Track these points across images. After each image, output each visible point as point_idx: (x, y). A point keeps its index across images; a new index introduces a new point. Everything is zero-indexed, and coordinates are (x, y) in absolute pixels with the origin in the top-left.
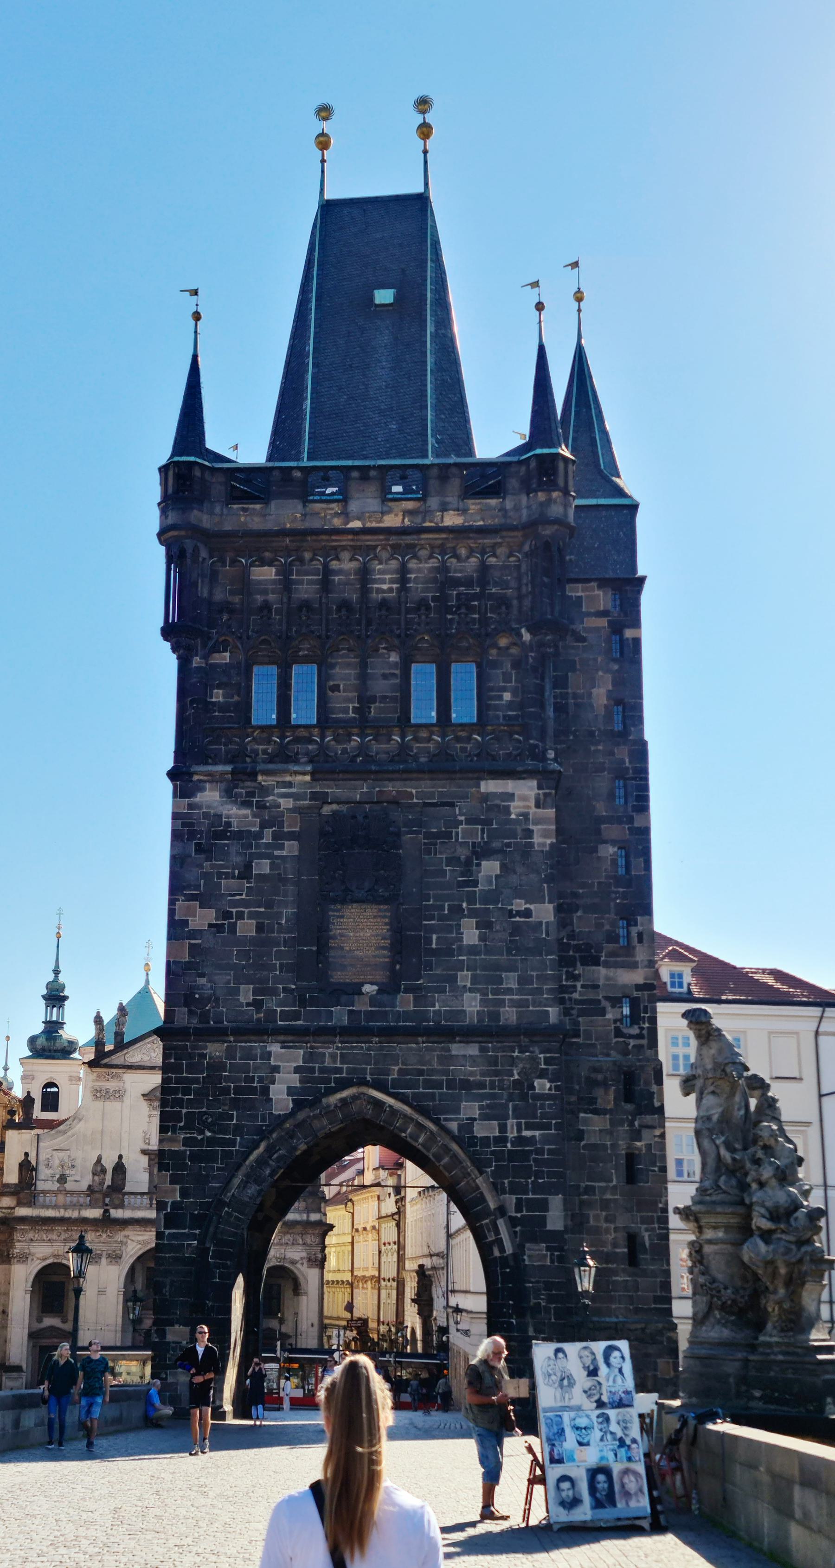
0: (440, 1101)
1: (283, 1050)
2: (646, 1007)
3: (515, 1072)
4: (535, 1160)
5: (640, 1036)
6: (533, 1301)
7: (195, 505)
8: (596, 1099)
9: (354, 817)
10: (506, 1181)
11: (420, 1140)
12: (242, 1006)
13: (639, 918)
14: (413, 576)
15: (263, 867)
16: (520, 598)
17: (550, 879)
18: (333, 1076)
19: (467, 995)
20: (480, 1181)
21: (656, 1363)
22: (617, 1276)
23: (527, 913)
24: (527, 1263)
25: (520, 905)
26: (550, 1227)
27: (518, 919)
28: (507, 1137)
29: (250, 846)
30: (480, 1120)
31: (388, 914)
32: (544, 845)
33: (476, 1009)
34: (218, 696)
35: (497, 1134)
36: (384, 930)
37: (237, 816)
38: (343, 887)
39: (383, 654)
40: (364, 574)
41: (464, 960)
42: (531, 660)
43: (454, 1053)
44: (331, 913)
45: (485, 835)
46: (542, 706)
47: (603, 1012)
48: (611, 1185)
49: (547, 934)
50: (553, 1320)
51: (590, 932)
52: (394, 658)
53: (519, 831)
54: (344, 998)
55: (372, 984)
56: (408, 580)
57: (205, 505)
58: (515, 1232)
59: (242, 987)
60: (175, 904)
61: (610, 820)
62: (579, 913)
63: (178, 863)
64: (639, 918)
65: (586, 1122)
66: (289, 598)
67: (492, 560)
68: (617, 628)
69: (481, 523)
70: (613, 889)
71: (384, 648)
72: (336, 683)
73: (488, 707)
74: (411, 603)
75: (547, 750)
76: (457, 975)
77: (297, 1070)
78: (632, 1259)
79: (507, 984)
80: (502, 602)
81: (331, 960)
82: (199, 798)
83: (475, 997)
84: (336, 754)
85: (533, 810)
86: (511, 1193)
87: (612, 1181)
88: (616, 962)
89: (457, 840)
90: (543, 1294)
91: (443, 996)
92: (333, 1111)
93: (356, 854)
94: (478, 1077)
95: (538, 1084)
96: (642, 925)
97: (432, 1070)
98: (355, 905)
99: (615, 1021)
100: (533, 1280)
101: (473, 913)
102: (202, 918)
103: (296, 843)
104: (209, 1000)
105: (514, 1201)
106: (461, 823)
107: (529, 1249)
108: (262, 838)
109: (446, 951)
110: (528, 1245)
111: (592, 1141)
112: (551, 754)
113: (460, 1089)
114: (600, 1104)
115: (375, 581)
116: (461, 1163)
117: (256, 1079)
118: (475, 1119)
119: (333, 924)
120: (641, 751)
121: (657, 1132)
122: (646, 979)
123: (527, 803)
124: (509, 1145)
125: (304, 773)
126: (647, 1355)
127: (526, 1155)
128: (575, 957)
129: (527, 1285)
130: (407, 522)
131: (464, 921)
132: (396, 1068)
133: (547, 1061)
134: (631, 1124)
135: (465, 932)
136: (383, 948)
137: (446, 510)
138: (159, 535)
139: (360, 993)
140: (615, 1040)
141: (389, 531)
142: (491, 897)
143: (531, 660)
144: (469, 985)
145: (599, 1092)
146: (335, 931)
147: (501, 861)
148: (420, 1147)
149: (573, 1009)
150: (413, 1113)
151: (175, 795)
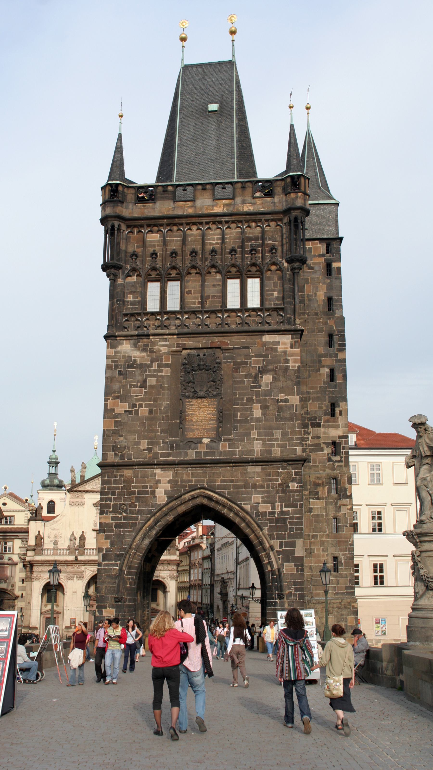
0: (241, 495)
1: (162, 472)
2: (343, 447)
5: (340, 461)
7: (119, 204)
8: (318, 492)
9: (198, 355)
18: (187, 484)
21: (346, 618)
31: (216, 403)
36: (214, 411)
38: (193, 390)
39: (214, 275)
40: (203, 237)
48: (325, 534)
51: (316, 411)
52: (219, 276)
54: (193, 445)
55: (207, 438)
57: (124, 204)
61: (325, 356)
62: (311, 402)
65: (314, 503)
66: (166, 249)
71: (213, 272)
72: (190, 290)
74: (227, 249)
77: (169, 482)
81: (186, 427)
84: (189, 325)
93: (199, 374)
97: (237, 480)
98: (199, 399)
99: (328, 454)
103: (169, 369)
111: (316, 513)
114: (320, 495)
115: (209, 239)
125: (173, 334)
126: (342, 615)
128: (308, 423)
132: (219, 479)
134: (336, 503)
136: (213, 420)
139: (201, 443)
146: (189, 411)
149: (307, 449)
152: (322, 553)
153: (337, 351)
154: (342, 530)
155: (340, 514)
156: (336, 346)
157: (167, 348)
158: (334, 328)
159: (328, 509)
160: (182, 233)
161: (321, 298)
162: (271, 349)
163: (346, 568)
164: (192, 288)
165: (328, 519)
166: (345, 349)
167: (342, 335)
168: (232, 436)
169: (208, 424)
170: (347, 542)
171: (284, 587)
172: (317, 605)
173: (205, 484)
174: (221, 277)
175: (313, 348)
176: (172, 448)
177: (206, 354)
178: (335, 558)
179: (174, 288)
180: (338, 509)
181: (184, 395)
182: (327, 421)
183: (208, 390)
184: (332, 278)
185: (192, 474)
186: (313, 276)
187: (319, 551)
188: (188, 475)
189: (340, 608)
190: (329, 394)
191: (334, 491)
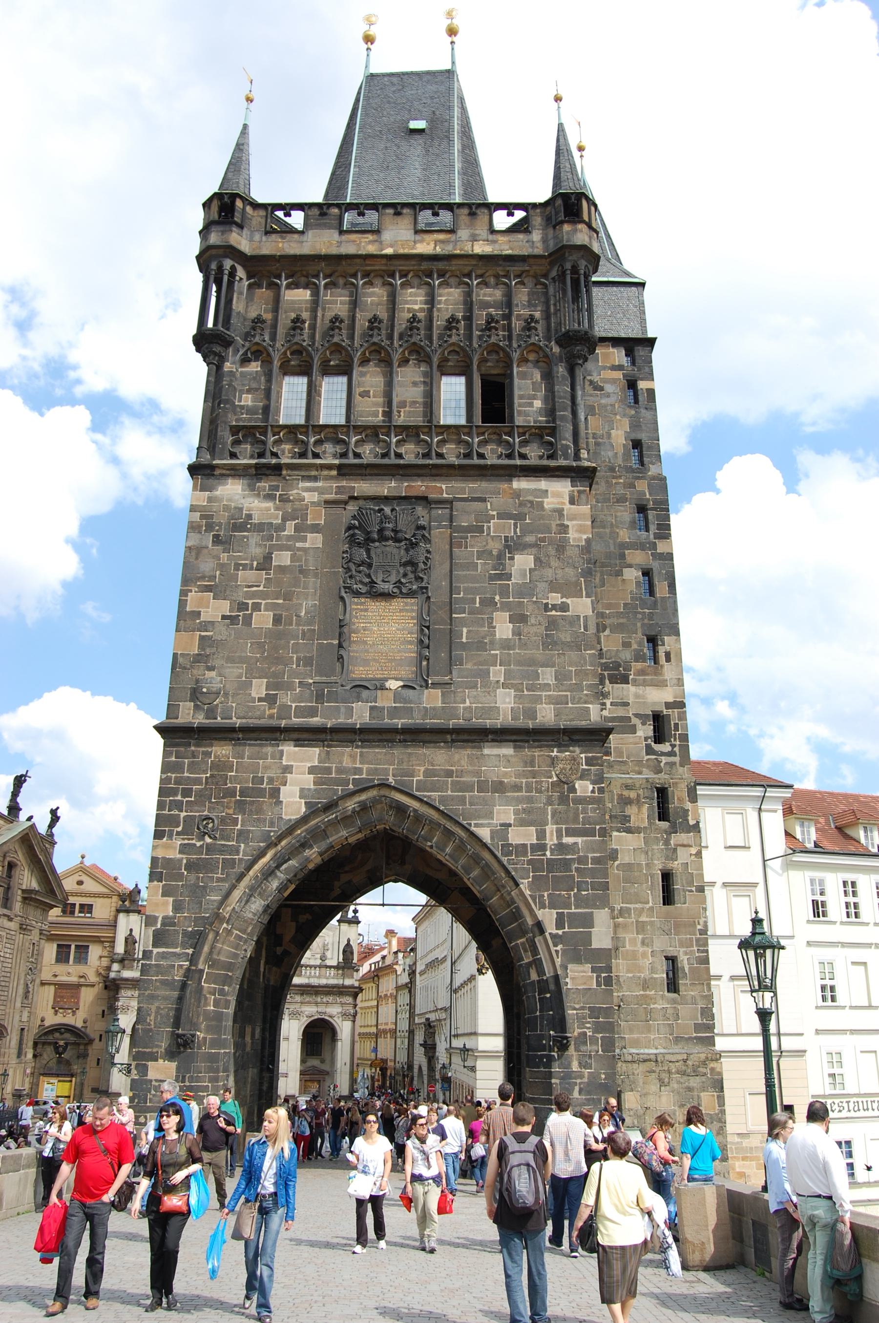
0: (471, 804)
2: (676, 725)
4: (577, 869)
8: (630, 816)
9: (381, 510)
10: (546, 894)
14: (444, 298)
15: (282, 558)
19: (500, 691)
22: (655, 1003)
23: (564, 607)
26: (595, 945)
27: (554, 613)
28: (545, 845)
29: (271, 538)
32: (580, 539)
33: (510, 706)
35: (535, 842)
36: (412, 624)
38: (368, 580)
47: (633, 730)
48: (647, 906)
49: (586, 628)
50: (600, 1052)
53: (554, 526)
54: (365, 694)
55: (397, 679)
56: (440, 302)
58: (557, 951)
60: (187, 596)
61: (633, 546)
62: (607, 632)
63: (193, 553)
68: (632, 385)
69: (509, 252)
76: (489, 669)
78: (673, 986)
83: (510, 693)
85: (567, 506)
86: (552, 906)
88: (644, 680)
89: (488, 534)
90: (589, 1022)
91: (474, 692)
92: (351, 816)
95: (580, 786)
99: (646, 739)
100: (577, 1006)
101: (506, 607)
102: (214, 609)
103: (319, 536)
106: (493, 517)
110: (570, 966)
111: (627, 860)
112: (584, 454)
115: (407, 302)
116: (494, 873)
118: (510, 825)
123: (561, 500)
124: (548, 853)
126: (690, 1089)
127: (566, 864)
129: (570, 1012)
130: (438, 250)
132: (422, 769)
133: (589, 762)
134: (667, 842)
136: (410, 643)
139: (383, 688)
141: (422, 257)
142: (526, 590)
144: (502, 680)
145: (631, 810)
147: (535, 555)
148: (447, 857)
150: (441, 818)
151: (195, 488)
152: (641, 950)
153: (655, 538)
154: (682, 899)
155: (675, 865)
156: (653, 528)
157: (316, 493)
158: (648, 496)
159: (650, 853)
161: (619, 441)
163: (692, 984)
164: (372, 386)
166: (670, 535)
167: (662, 510)
169: (399, 651)
170: (694, 925)
171: (569, 1021)
172: (635, 1066)
173: (391, 780)
174: (429, 369)
175: (608, 531)
178: (672, 960)
179: (333, 389)
180: (672, 853)
181: (348, 589)
182: (642, 672)
184: (638, 408)
185: (362, 754)
186: (603, 401)
187: (636, 945)
188: (353, 757)
189: (684, 1073)
190: (643, 619)
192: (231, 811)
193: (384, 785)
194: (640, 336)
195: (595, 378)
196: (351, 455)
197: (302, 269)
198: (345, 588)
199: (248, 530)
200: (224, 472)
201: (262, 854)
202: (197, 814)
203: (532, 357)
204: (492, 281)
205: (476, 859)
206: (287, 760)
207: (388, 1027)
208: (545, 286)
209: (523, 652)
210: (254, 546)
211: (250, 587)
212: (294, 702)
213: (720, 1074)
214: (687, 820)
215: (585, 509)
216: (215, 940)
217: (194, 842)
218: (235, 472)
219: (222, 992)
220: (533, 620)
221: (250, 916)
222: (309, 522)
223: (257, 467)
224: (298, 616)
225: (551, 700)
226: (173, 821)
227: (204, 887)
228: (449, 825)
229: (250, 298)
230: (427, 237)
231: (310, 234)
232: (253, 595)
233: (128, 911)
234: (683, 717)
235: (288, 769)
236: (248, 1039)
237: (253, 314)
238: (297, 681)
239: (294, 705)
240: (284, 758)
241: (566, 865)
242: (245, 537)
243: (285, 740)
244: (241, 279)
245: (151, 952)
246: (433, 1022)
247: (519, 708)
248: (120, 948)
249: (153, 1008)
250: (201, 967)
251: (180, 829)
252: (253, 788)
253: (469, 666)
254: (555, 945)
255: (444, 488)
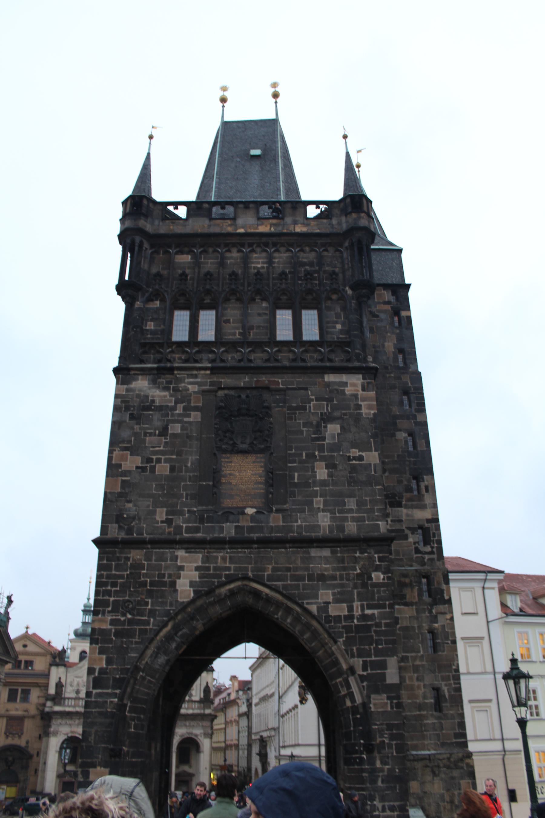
0: (303, 589)
2: (434, 534)
3: (357, 568)
4: (375, 631)
5: (432, 553)
6: (379, 740)
8: (406, 595)
9: (239, 397)
10: (355, 648)
11: (289, 620)
12: (157, 522)
13: (425, 477)
15: (176, 428)
16: (344, 272)
17: (375, 436)
18: (224, 573)
19: (320, 514)
20: (334, 648)
21: (459, 784)
22: (427, 719)
23: (361, 458)
24: (372, 710)
25: (356, 452)
26: (389, 681)
27: (354, 462)
29: (167, 415)
30: (333, 603)
31: (263, 460)
32: (369, 414)
33: (327, 524)
34: (151, 326)
36: (261, 471)
37: (160, 396)
38: (231, 442)
41: (317, 490)
42: (353, 305)
43: (313, 554)
44: (223, 460)
45: (329, 408)
46: (362, 332)
47: (406, 537)
48: (419, 654)
49: (375, 472)
52: (264, 304)
53: (352, 406)
54: (231, 517)
55: (252, 507)
56: (274, 263)
58: (363, 686)
59: (158, 510)
60: (112, 453)
61: (401, 417)
63: (117, 426)
64: (425, 477)
66: (199, 272)
67: (325, 253)
68: (396, 312)
69: (318, 231)
70: (407, 459)
72: (228, 318)
73: (327, 333)
75: (367, 356)
79: (348, 506)
80: (333, 275)
81: (222, 491)
82: (133, 385)
85: (360, 392)
86: (359, 656)
87: (419, 652)
90: (386, 734)
91: (303, 515)
94: (331, 572)
95: (375, 576)
96: (427, 481)
99: (415, 543)
100: (378, 723)
102: (132, 462)
103: (199, 414)
104: (134, 518)
105: (361, 662)
106: (312, 400)
107: (374, 699)
108: (176, 410)
109: (305, 484)
110: (373, 696)
111: (405, 624)
112: (370, 359)
113: (318, 581)
114: (408, 599)
115: (253, 263)
117: (166, 575)
118: (329, 603)
119: (225, 467)
120: (418, 377)
121: (448, 616)
122: (433, 515)
123: (356, 388)
124: (355, 621)
125: (205, 369)
126: (453, 778)
127: (368, 628)
130: (272, 229)
131: (317, 464)
132: (270, 567)
133: (380, 559)
134: (430, 612)
135: (318, 471)
137: (297, 224)
138: (120, 236)
139: (243, 513)
140: (415, 556)
141: (262, 235)
143: (353, 305)
144: (322, 507)
145: (407, 591)
146: (226, 470)
148: (288, 625)
151: (117, 383)
156: (414, 406)
158: (410, 385)
159: (420, 619)
160: (219, 256)
162: (336, 391)
165: (422, 634)
168: (288, 505)
170: (450, 666)
172: (416, 763)
173: (250, 574)
174: (268, 305)
176: (202, 520)
177: (250, 395)
178: (437, 690)
180: (434, 619)
181: (219, 449)
182: (410, 500)
183: (252, 443)
186: (379, 324)
188: (224, 559)
191: (426, 595)
192: (144, 597)
193: (246, 578)
194: (401, 283)
195: (374, 309)
196: (218, 360)
197: (185, 241)
198: (217, 447)
199: (151, 410)
200: (136, 372)
201: (165, 625)
202: (121, 599)
203: (334, 297)
204: (307, 249)
205: (308, 626)
206: (181, 562)
207: (232, 743)
208: (341, 252)
209: (335, 488)
210: (157, 421)
211: (153, 447)
212: (183, 523)
213: (473, 767)
214: (444, 597)
215: (372, 394)
216: (135, 684)
217: (119, 617)
218: (144, 372)
219: (139, 719)
220: (340, 467)
221: (157, 667)
222: (192, 405)
223: (158, 369)
224: (186, 466)
225: (354, 519)
226: (106, 603)
227: (127, 648)
228: (289, 604)
229: (152, 261)
230: (264, 221)
231: (191, 221)
232: (156, 453)
233: (57, 665)
234: (438, 528)
235: (182, 568)
236: (153, 751)
237: (154, 270)
238: (186, 509)
239: (184, 525)
240: (179, 561)
241: (368, 628)
242: (150, 414)
243: (179, 549)
244: (146, 249)
245: (91, 692)
246: (265, 738)
247: (333, 525)
248: (52, 691)
249: (93, 731)
250: (125, 702)
251: (110, 609)
252: (158, 581)
253: (300, 498)
254: (362, 682)
255: (280, 381)
